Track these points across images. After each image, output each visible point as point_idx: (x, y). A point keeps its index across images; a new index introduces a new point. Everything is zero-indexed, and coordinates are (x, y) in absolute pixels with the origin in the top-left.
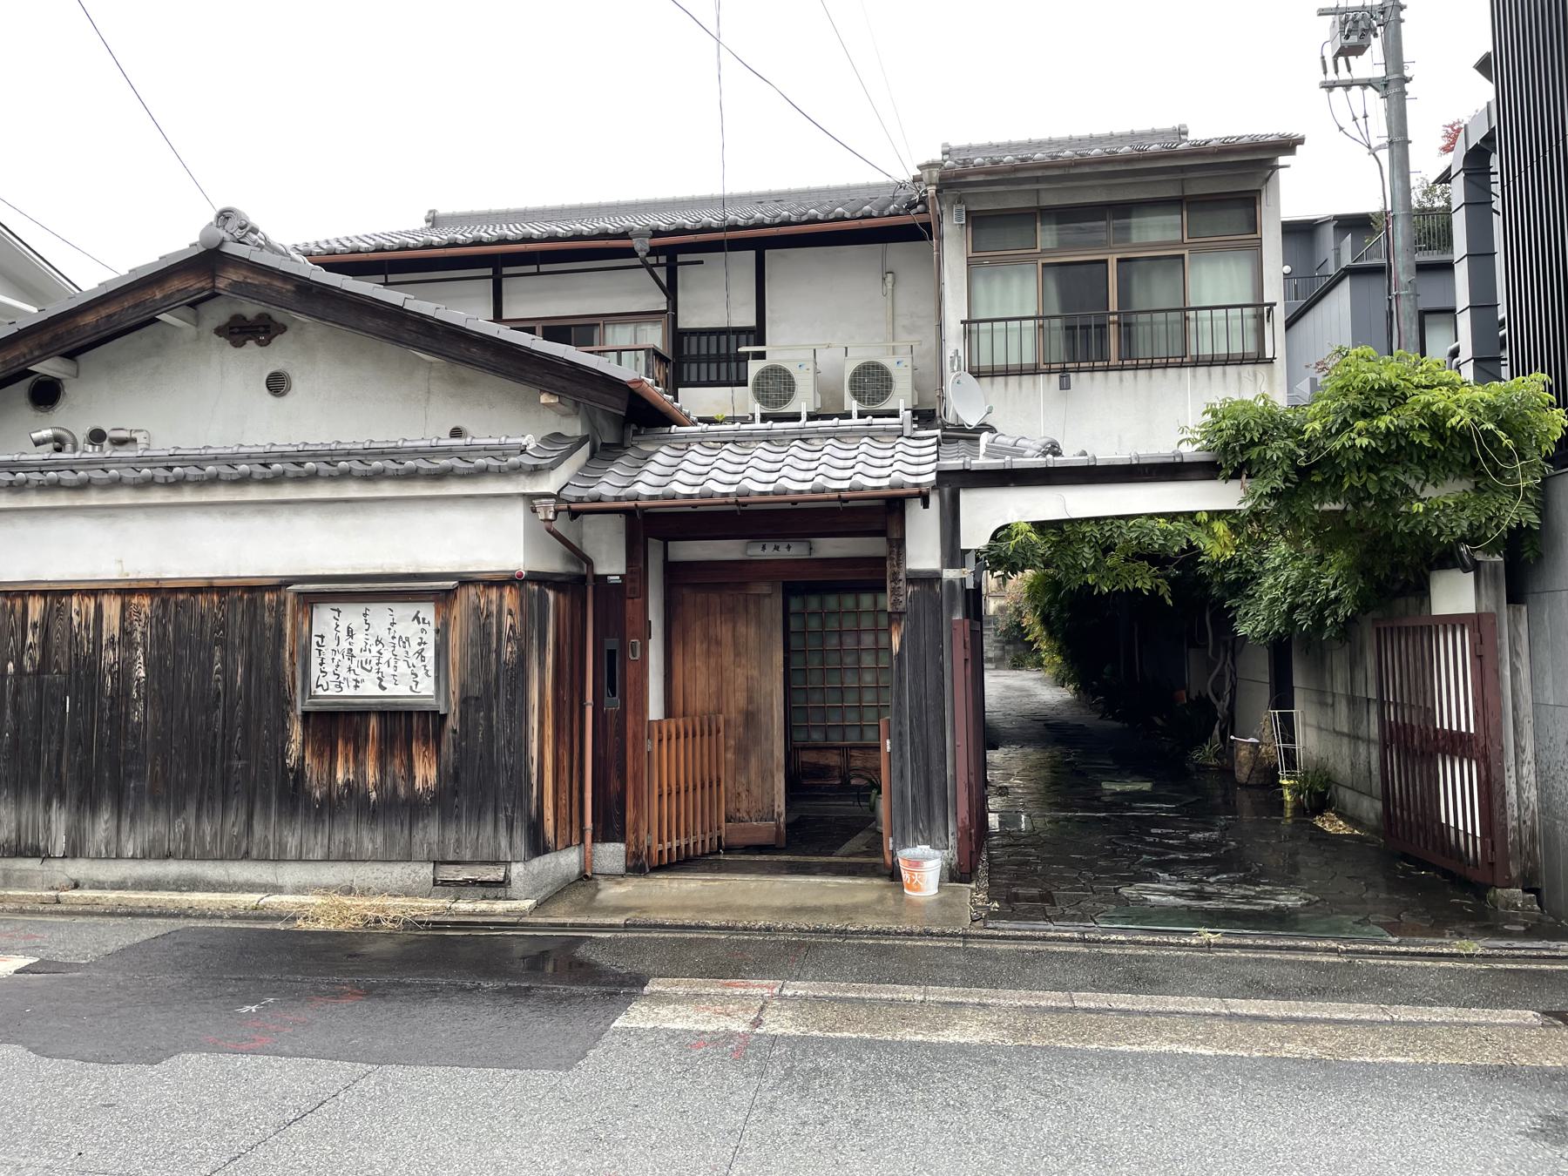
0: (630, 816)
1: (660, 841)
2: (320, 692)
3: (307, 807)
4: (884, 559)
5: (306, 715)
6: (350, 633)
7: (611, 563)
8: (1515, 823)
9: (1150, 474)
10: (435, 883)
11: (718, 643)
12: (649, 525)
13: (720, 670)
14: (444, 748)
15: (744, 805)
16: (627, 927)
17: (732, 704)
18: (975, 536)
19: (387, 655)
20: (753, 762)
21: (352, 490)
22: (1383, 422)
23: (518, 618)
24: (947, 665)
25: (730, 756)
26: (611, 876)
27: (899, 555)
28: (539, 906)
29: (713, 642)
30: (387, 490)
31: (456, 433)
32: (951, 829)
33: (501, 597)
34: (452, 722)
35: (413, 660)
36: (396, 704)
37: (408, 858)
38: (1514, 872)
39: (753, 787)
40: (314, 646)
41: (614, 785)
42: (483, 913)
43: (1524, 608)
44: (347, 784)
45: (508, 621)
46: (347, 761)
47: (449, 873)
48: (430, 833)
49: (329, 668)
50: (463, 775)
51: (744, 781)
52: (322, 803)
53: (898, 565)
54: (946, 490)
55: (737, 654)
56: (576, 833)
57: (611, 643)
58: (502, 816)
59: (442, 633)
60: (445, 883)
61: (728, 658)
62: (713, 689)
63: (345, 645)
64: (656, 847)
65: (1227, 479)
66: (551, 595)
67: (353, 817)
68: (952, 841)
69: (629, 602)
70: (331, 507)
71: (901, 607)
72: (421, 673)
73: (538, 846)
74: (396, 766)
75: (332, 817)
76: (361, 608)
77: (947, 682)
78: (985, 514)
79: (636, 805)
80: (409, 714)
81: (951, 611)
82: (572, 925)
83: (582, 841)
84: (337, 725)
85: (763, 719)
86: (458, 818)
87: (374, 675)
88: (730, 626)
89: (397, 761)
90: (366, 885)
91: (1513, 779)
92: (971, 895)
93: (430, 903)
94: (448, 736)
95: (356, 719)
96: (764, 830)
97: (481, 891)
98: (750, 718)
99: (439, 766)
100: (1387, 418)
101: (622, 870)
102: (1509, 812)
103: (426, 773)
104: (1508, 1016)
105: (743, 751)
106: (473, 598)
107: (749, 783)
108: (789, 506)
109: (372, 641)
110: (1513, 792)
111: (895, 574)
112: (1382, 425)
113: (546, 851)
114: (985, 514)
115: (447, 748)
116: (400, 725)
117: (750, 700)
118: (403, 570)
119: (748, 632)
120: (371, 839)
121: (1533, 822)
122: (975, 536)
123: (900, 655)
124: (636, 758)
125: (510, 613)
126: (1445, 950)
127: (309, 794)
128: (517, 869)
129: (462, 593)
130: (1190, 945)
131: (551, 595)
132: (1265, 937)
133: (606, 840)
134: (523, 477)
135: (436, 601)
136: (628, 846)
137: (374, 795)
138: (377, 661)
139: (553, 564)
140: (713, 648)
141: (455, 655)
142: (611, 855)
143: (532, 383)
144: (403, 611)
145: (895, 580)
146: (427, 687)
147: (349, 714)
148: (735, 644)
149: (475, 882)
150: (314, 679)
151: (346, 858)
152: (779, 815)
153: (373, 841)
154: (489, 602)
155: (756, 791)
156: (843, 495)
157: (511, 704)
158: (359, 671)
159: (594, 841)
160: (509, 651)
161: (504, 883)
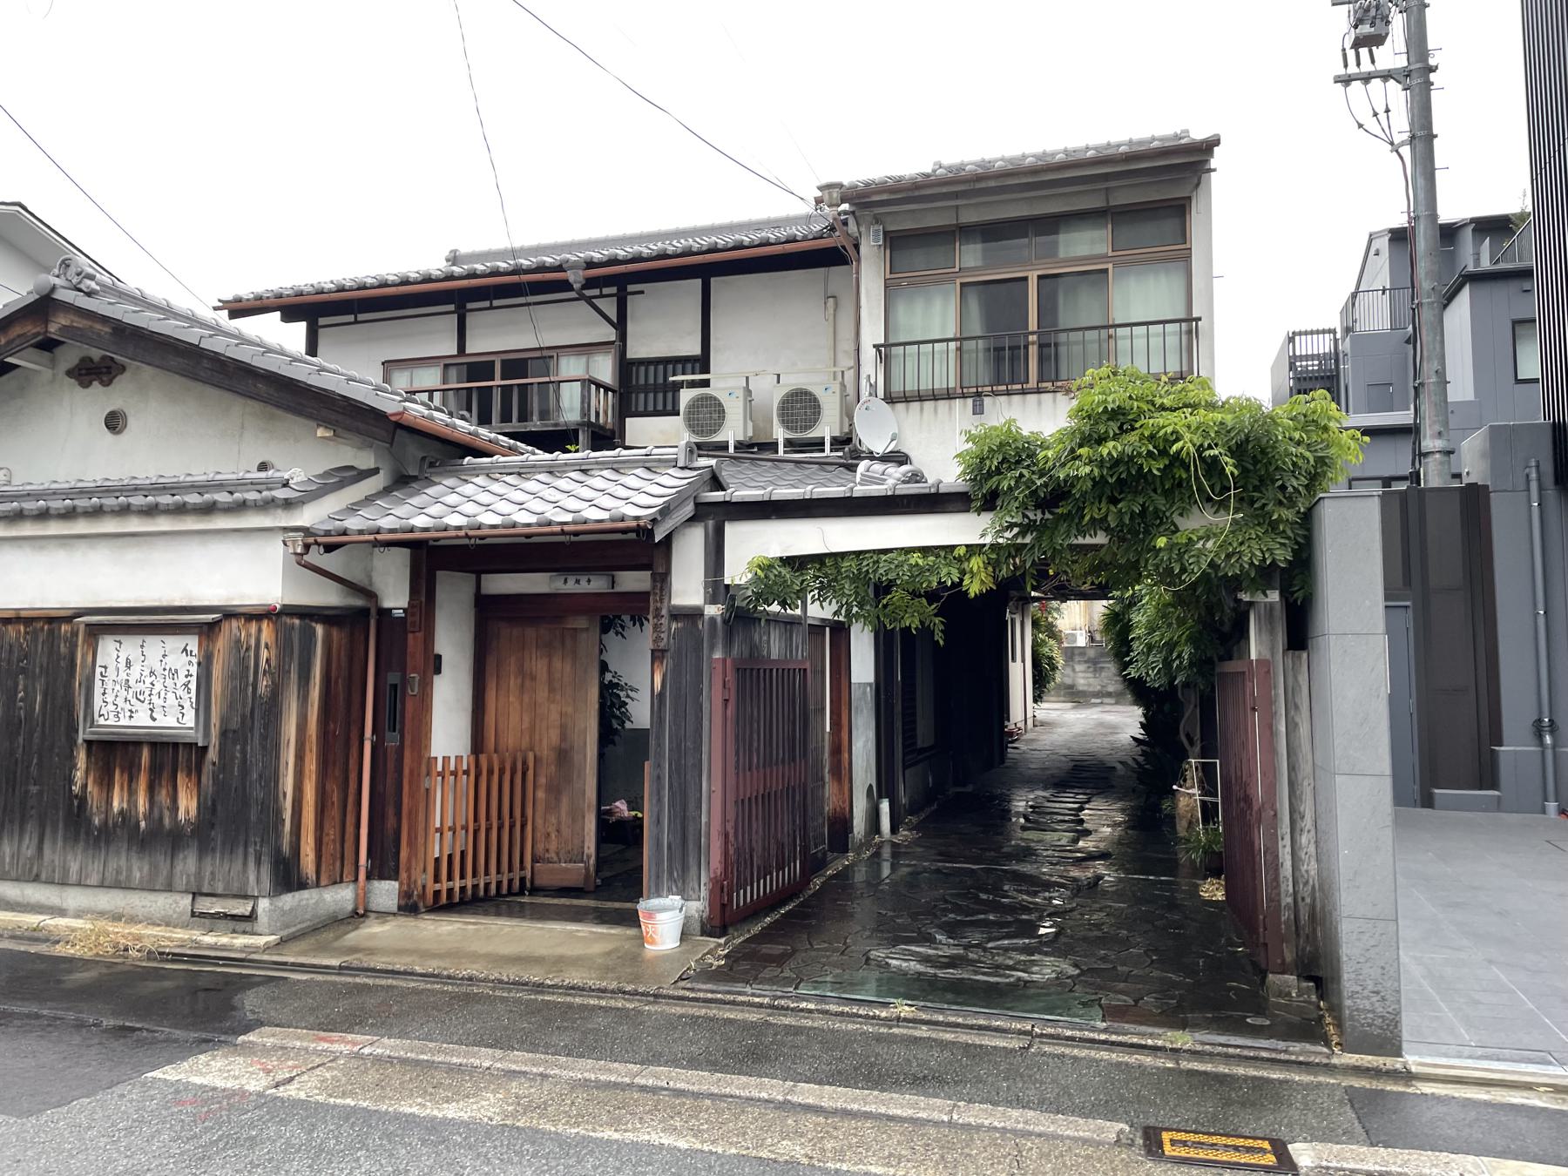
0: (404, 854)
1: (437, 879)
2: (102, 721)
3: (88, 833)
4: (647, 594)
5: (89, 743)
6: (128, 664)
7: (396, 597)
8: (1290, 900)
9: (908, 506)
10: (193, 914)
11: (533, 678)
12: (432, 557)
13: (534, 705)
14: (204, 779)
15: (553, 846)
16: (341, 970)
17: (545, 742)
18: (737, 571)
19: (158, 687)
20: (565, 801)
21: (134, 525)
22: (1109, 448)
23: (273, 652)
24: (705, 705)
25: (541, 794)
26: (383, 915)
27: (662, 590)
28: (283, 942)
29: (526, 676)
30: (164, 524)
31: (263, 467)
32: (703, 879)
33: (260, 630)
34: (212, 755)
35: (180, 692)
36: (161, 735)
37: (169, 888)
38: (1289, 956)
39: (563, 827)
40: (98, 676)
41: (391, 821)
42: (223, 948)
43: (1305, 655)
44: (121, 812)
45: (264, 654)
46: (122, 789)
47: (206, 905)
48: (188, 863)
49: (110, 699)
50: (219, 808)
51: (554, 820)
52: (100, 831)
53: (661, 601)
54: (711, 523)
55: (552, 690)
56: (348, 868)
57: (393, 678)
58: (251, 850)
59: (205, 666)
60: (203, 915)
61: (542, 693)
62: (526, 725)
63: (123, 676)
64: (431, 887)
65: (979, 511)
66: (320, 630)
67: (125, 846)
68: (704, 893)
69: (410, 636)
70: (120, 541)
71: (662, 645)
72: (187, 705)
73: (288, 878)
74: (163, 796)
75: (108, 843)
76: (138, 639)
77: (706, 723)
78: (753, 547)
79: (411, 844)
80: (176, 745)
81: (712, 648)
82: (293, 964)
83: (356, 880)
84: (116, 753)
85: (577, 758)
86: (213, 850)
87: (146, 706)
88: (545, 661)
89: (164, 792)
90: (133, 912)
91: (1288, 849)
92: (715, 950)
93: (180, 934)
94: (207, 769)
95: (131, 748)
96: (574, 872)
97: (231, 924)
98: (564, 756)
99: (206, 802)
100: (1111, 444)
101: (395, 909)
102: (1283, 887)
103: (187, 805)
104: (1084, 1128)
105: (555, 790)
106: (235, 631)
107: (559, 823)
108: (523, 540)
109: (146, 673)
110: (1288, 864)
111: (658, 610)
112: (1105, 452)
113: (302, 885)
114: (753, 547)
115: (206, 779)
116: (168, 756)
117: (563, 737)
118: (177, 603)
119: (563, 667)
120: (139, 869)
121: (1314, 900)
122: (737, 571)
123: (662, 695)
124: (412, 796)
125: (267, 646)
126: (1150, 1042)
127: (89, 821)
128: (264, 904)
129: (225, 626)
130: (879, 1018)
131: (320, 630)
132: (957, 1013)
133: (382, 877)
134: (279, 511)
135: (200, 634)
136: (401, 884)
137: (143, 824)
138: (148, 690)
139: (327, 596)
140: (528, 683)
141: (217, 687)
142: (386, 893)
143: (310, 417)
144: (174, 643)
145: (658, 615)
146: (189, 720)
147: (126, 744)
148: (550, 681)
149: (226, 916)
150: (96, 709)
151: (118, 885)
152: (589, 857)
153: (141, 870)
154: (249, 635)
155: (566, 831)
156: (566, 528)
157: (264, 737)
158: (134, 701)
159: (369, 877)
160: (264, 683)
161: (251, 917)
